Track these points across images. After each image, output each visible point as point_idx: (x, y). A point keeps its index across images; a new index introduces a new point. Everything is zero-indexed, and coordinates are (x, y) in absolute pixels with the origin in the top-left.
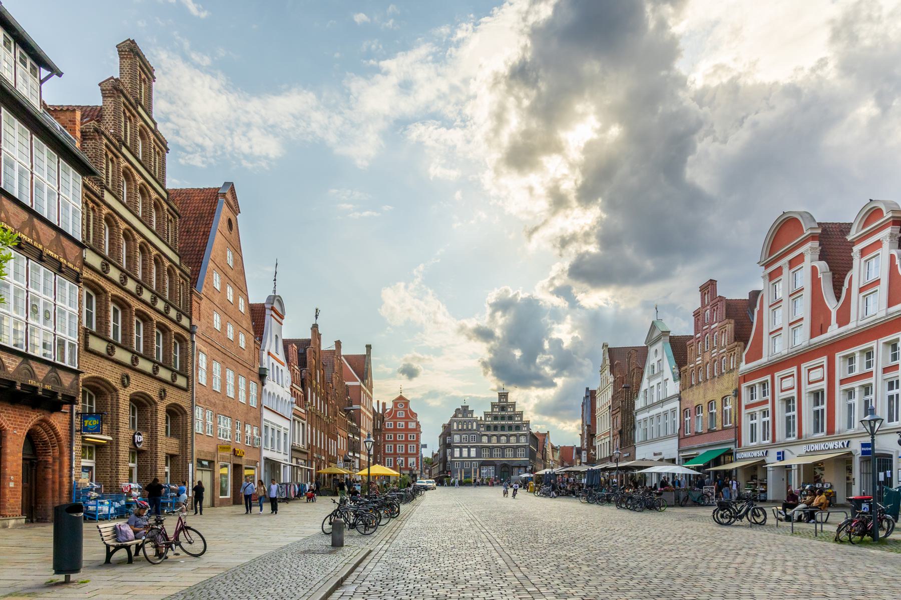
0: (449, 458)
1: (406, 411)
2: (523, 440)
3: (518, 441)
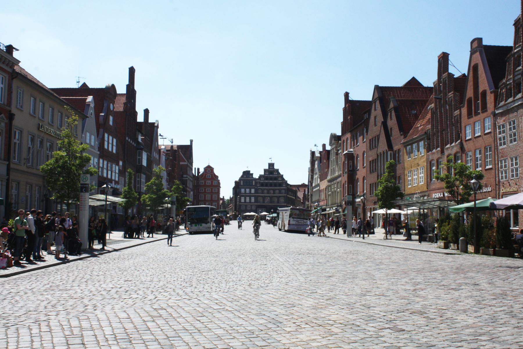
1: (212, 175)
2: (283, 191)
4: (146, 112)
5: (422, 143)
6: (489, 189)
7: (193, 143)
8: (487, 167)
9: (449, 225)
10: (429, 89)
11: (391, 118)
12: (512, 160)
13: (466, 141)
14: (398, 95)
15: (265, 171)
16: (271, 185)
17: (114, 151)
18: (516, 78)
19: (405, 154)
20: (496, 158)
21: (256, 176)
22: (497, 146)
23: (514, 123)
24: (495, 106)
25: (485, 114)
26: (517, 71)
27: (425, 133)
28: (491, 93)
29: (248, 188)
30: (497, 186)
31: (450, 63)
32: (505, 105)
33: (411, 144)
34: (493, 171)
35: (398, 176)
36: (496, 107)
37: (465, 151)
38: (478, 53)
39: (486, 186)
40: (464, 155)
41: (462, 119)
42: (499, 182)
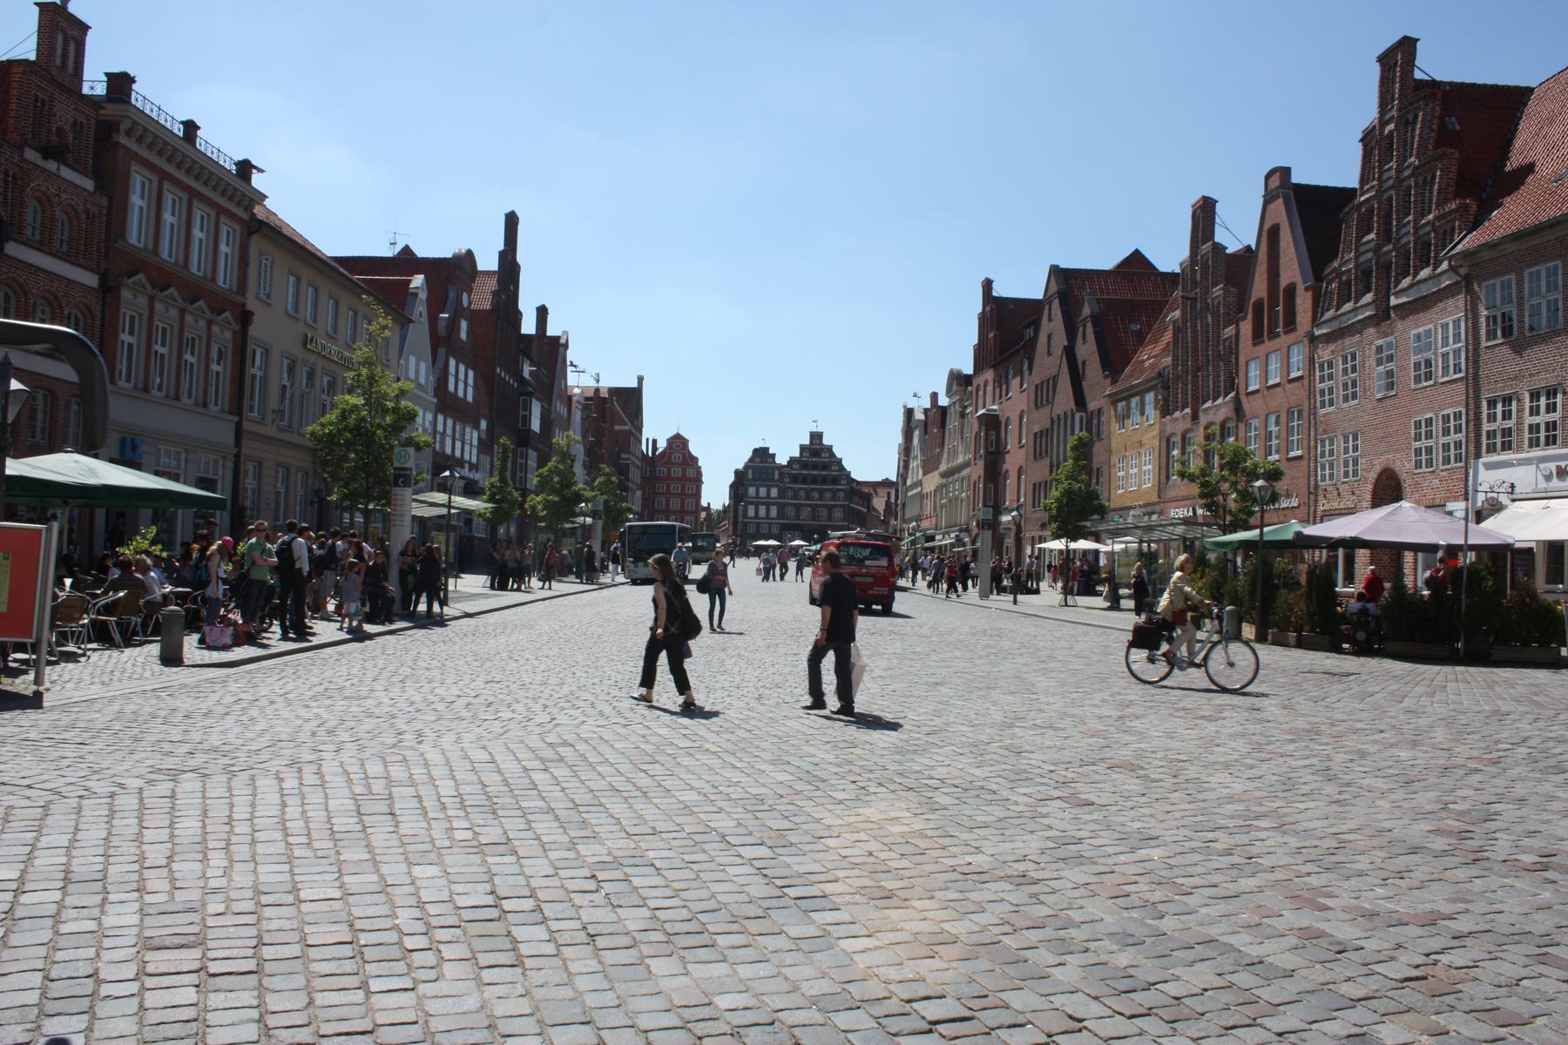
1: (684, 455)
2: (842, 495)
4: (542, 312)
5: (1150, 397)
6: (1294, 502)
8: (1292, 454)
9: (1202, 578)
10: (1172, 278)
11: (1084, 338)
12: (1346, 440)
13: (1248, 394)
14: (1101, 289)
15: (803, 448)
16: (814, 480)
17: (470, 398)
18: (1362, 259)
19: (1113, 420)
20: (1312, 433)
21: (782, 460)
22: (1315, 408)
23: (1354, 358)
24: (1314, 319)
25: (1291, 337)
26: (1366, 243)
27: (1159, 374)
28: (1306, 289)
29: (763, 486)
30: (1312, 497)
31: (1217, 220)
32: (1335, 318)
33: (1127, 399)
34: (1304, 463)
35: (1095, 467)
36: (1315, 321)
37: (1244, 416)
38: (1281, 201)
39: (1288, 496)
40: (1241, 426)
41: (1241, 346)
42: (1316, 486)
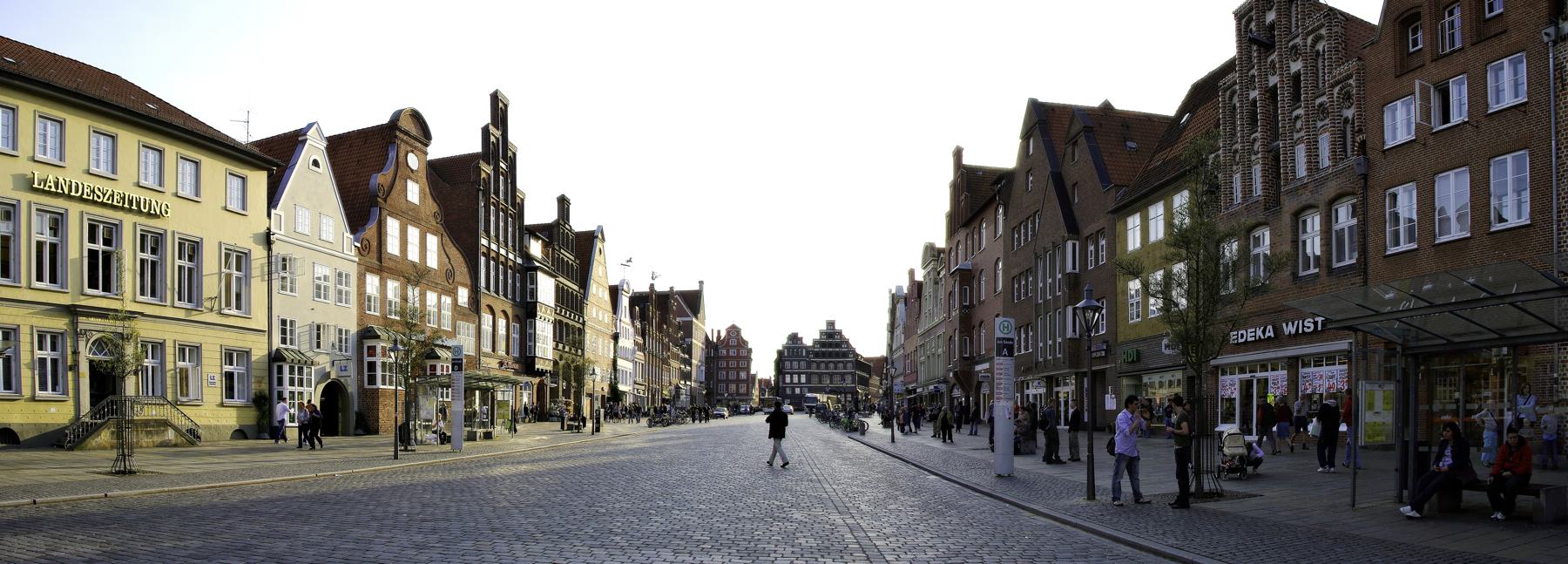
0: (781, 384)
2: (849, 365)
3: (845, 368)
4: (563, 203)
7: (705, 286)
15: (822, 333)
16: (830, 355)
21: (808, 342)
